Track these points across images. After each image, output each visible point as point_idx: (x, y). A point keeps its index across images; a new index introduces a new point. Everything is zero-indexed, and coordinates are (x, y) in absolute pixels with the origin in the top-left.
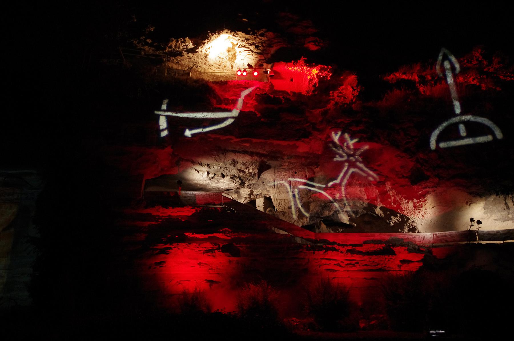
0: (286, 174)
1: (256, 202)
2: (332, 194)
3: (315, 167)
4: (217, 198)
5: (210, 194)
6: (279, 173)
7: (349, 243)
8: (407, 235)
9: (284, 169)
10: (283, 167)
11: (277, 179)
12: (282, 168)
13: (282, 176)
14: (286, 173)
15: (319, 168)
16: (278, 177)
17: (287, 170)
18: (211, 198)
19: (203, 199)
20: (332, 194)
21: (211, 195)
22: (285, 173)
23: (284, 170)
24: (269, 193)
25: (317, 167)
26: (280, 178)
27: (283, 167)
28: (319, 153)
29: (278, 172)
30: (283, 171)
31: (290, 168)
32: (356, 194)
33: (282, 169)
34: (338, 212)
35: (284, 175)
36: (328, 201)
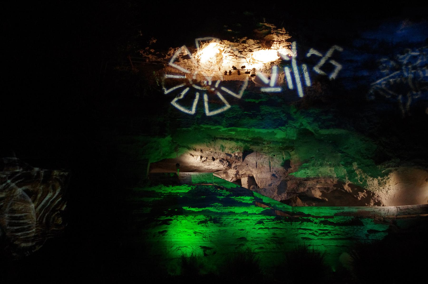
1: (241, 181)
2: (306, 173)
3: (291, 150)
4: (208, 178)
5: (203, 175)
6: (260, 156)
7: (322, 215)
8: (373, 208)
9: (264, 152)
10: (264, 151)
11: (258, 161)
12: (263, 152)
13: (262, 159)
14: (266, 156)
15: (294, 151)
16: (260, 159)
17: (267, 154)
18: (203, 178)
19: (197, 178)
20: (306, 173)
21: (204, 175)
22: (265, 156)
23: (264, 154)
24: (252, 173)
25: (293, 151)
27: (264, 151)
28: (294, 139)
29: (260, 155)
30: (263, 154)
31: (270, 151)
32: (327, 173)
33: (262, 153)
34: (311, 189)
35: (264, 158)
36: (302, 179)
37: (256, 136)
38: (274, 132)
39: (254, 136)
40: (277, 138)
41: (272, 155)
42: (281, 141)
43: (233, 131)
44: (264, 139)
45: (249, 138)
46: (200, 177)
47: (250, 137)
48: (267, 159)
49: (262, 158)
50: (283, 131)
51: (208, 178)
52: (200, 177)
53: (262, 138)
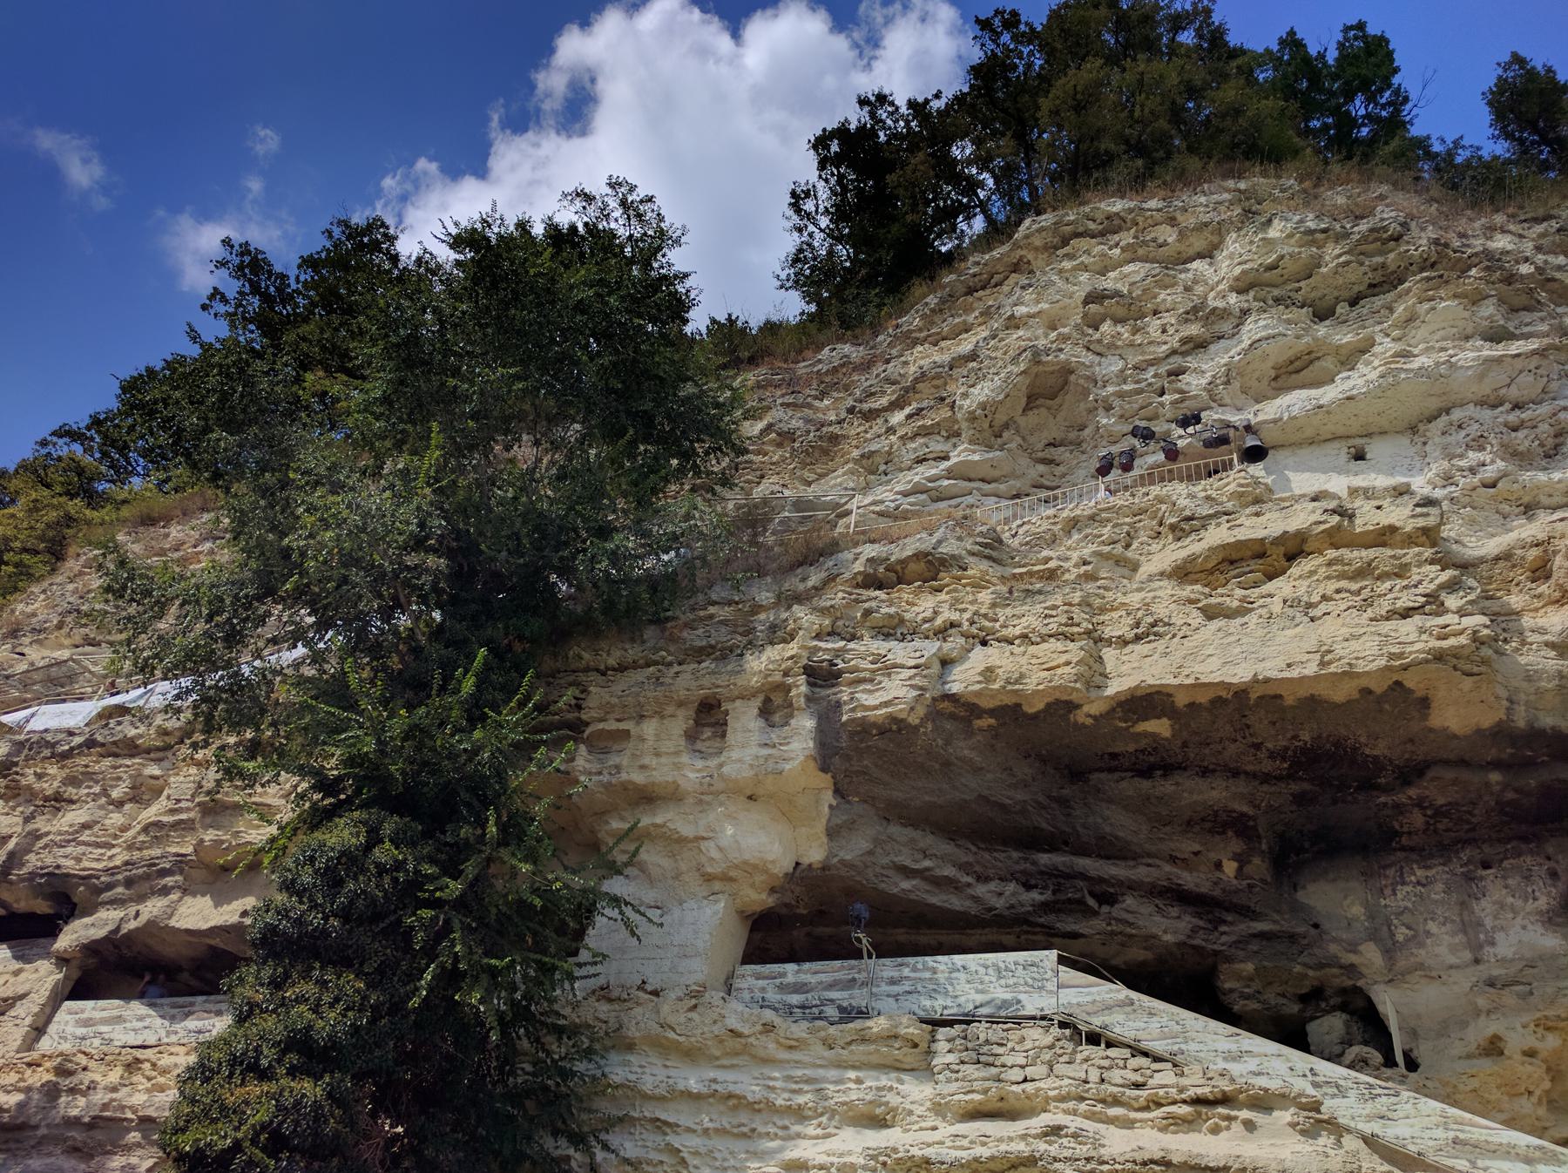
0: (1430, 873)
4: (1030, 982)
5: (1002, 965)
6: (1391, 872)
9: (1412, 849)
10: (1405, 840)
11: (1383, 902)
12: (1403, 849)
13: (1409, 888)
16: (1388, 892)
17: (1431, 856)
18: (1003, 982)
22: (1420, 873)
23: (1414, 856)
26: (1399, 896)
27: (1405, 840)
29: (1385, 867)
35: (1419, 883)
37: (1306, 736)
38: (1410, 691)
39: (1295, 737)
40: (1455, 736)
41: (1469, 862)
42: (1492, 754)
43: (1159, 718)
44: (1367, 751)
45: (1272, 755)
46: (987, 978)
47: (1270, 745)
48: (1440, 886)
49: (1404, 883)
50: (1467, 667)
51: (1030, 982)
52: (987, 978)
53: (1355, 749)
